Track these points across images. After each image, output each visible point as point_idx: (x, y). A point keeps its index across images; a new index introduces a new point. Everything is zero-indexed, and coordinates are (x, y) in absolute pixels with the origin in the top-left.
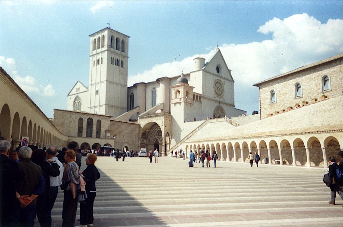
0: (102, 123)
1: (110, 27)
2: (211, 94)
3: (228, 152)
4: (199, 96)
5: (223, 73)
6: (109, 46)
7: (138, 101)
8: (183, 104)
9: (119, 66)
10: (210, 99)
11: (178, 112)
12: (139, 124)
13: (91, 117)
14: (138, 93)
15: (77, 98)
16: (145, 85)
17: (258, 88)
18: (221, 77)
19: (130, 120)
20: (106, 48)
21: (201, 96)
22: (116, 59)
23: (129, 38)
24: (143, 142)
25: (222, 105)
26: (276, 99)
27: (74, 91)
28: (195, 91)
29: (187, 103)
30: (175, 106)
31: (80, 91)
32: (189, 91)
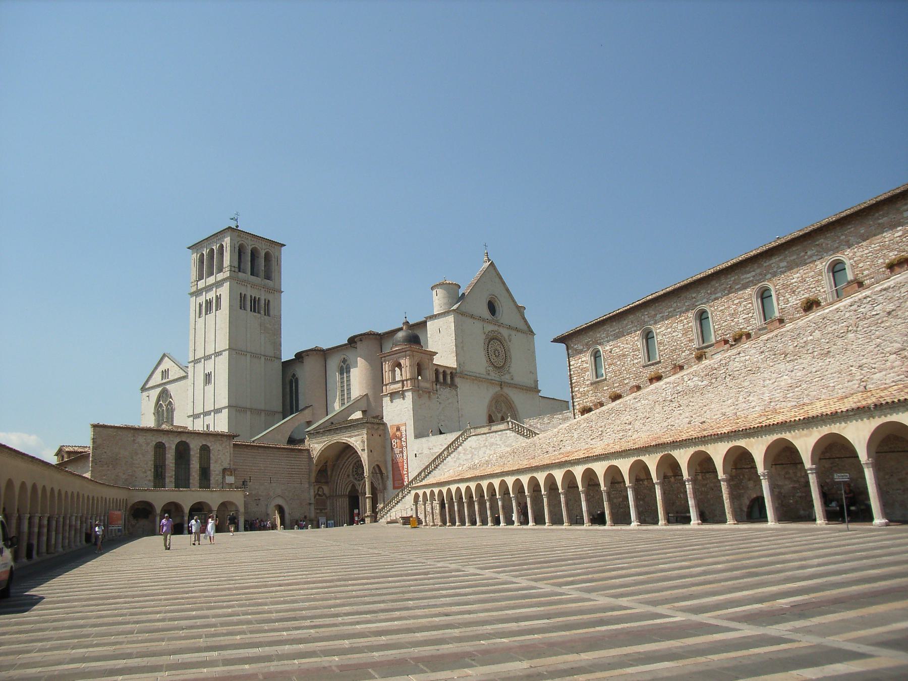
0: (212, 452)
1: (237, 226)
2: (479, 364)
3: (500, 503)
4: (448, 372)
5: (506, 314)
7: (307, 392)
8: (409, 395)
9: (259, 312)
10: (476, 379)
11: (398, 413)
12: (308, 450)
13: (184, 438)
14: (307, 374)
15: (165, 394)
16: (323, 354)
17: (563, 346)
18: (501, 325)
19: (291, 441)
20: (226, 274)
23: (283, 248)
26: (606, 369)
27: (157, 379)
28: (437, 360)
30: (392, 401)
31: (171, 378)
32: (422, 361)
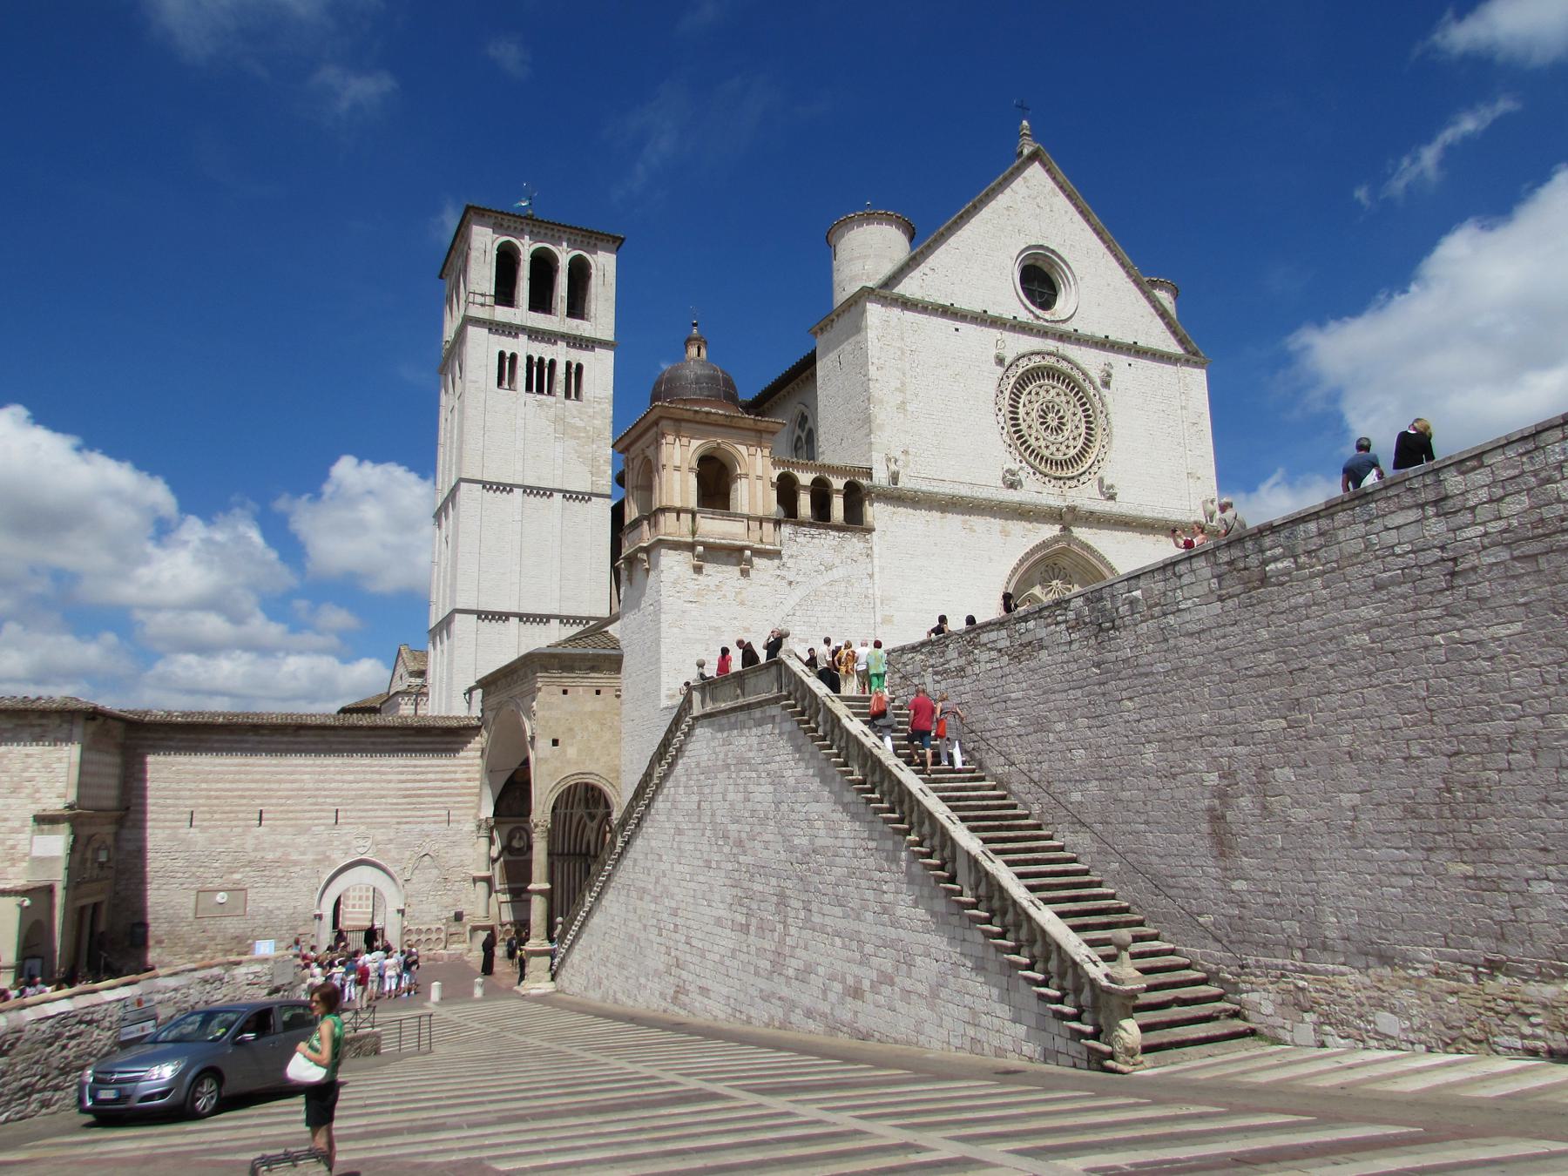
4: (838, 483)
6: (479, 299)
21: (864, 482)
22: (530, 359)
24: (516, 844)
25: (1081, 533)
29: (700, 549)
